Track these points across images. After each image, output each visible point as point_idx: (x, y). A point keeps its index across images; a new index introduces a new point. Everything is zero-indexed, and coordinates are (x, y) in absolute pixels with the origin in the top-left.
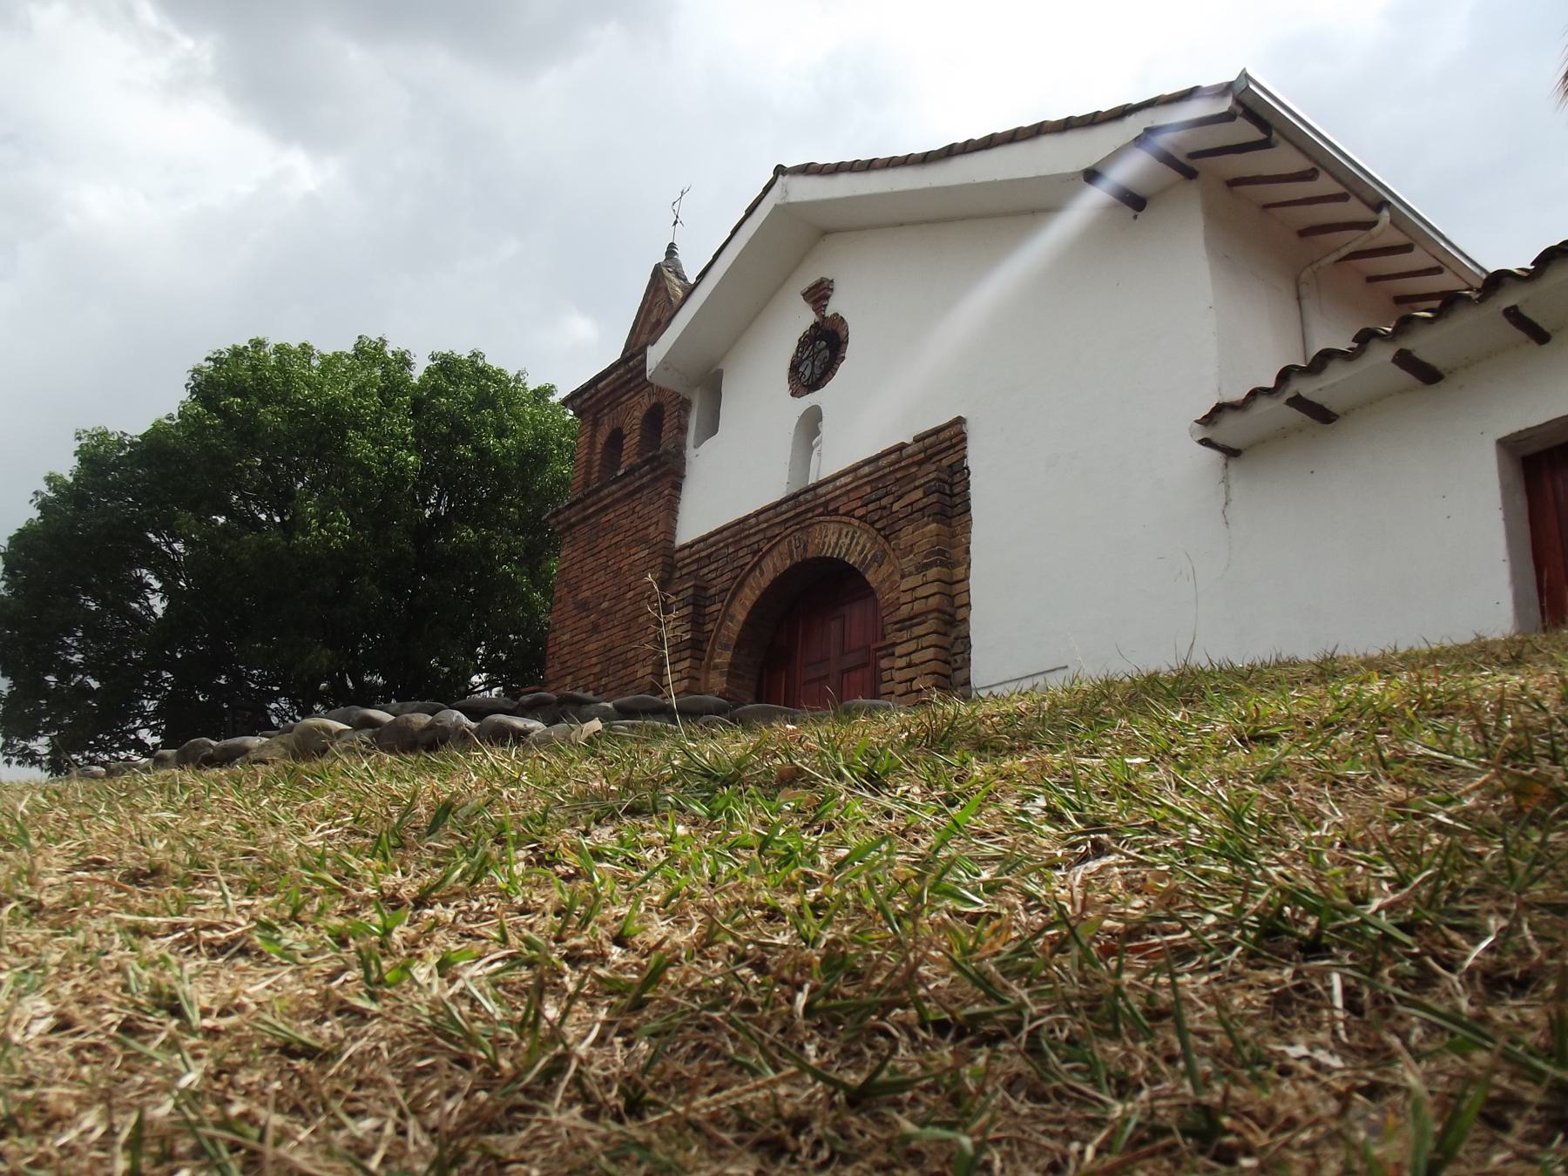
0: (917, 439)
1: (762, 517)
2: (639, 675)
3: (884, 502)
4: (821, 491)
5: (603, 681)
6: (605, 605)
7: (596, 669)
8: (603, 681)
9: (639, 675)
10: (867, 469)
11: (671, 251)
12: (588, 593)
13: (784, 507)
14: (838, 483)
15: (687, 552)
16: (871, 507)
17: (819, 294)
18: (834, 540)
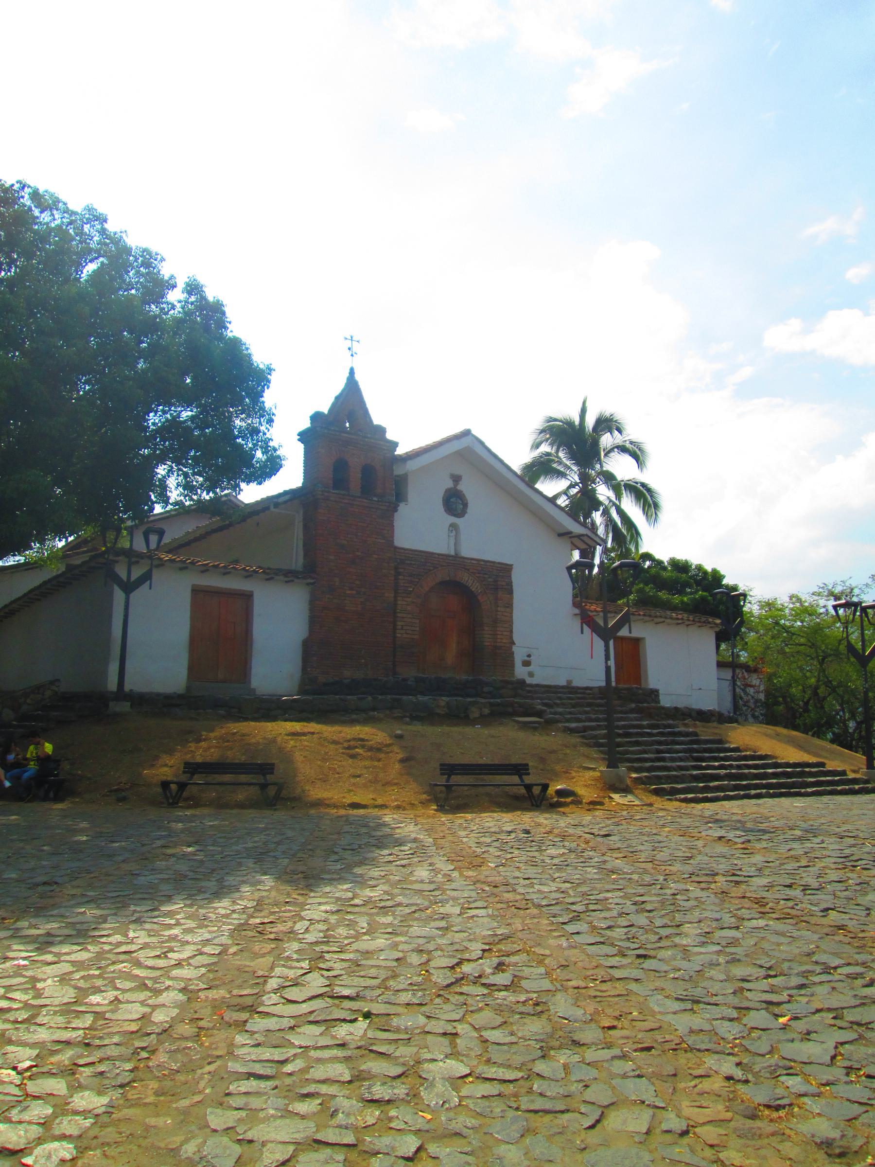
0: (499, 563)
1: (441, 557)
2: (386, 595)
3: (486, 576)
4: (466, 561)
5: (363, 590)
6: (359, 554)
7: (358, 582)
8: (363, 590)
9: (386, 595)
10: (482, 563)
11: (352, 372)
12: (346, 542)
13: (451, 558)
14: (473, 562)
15: (402, 551)
16: (482, 575)
17: (457, 479)
18: (466, 579)
